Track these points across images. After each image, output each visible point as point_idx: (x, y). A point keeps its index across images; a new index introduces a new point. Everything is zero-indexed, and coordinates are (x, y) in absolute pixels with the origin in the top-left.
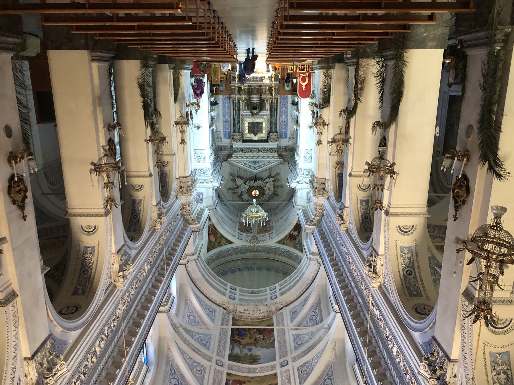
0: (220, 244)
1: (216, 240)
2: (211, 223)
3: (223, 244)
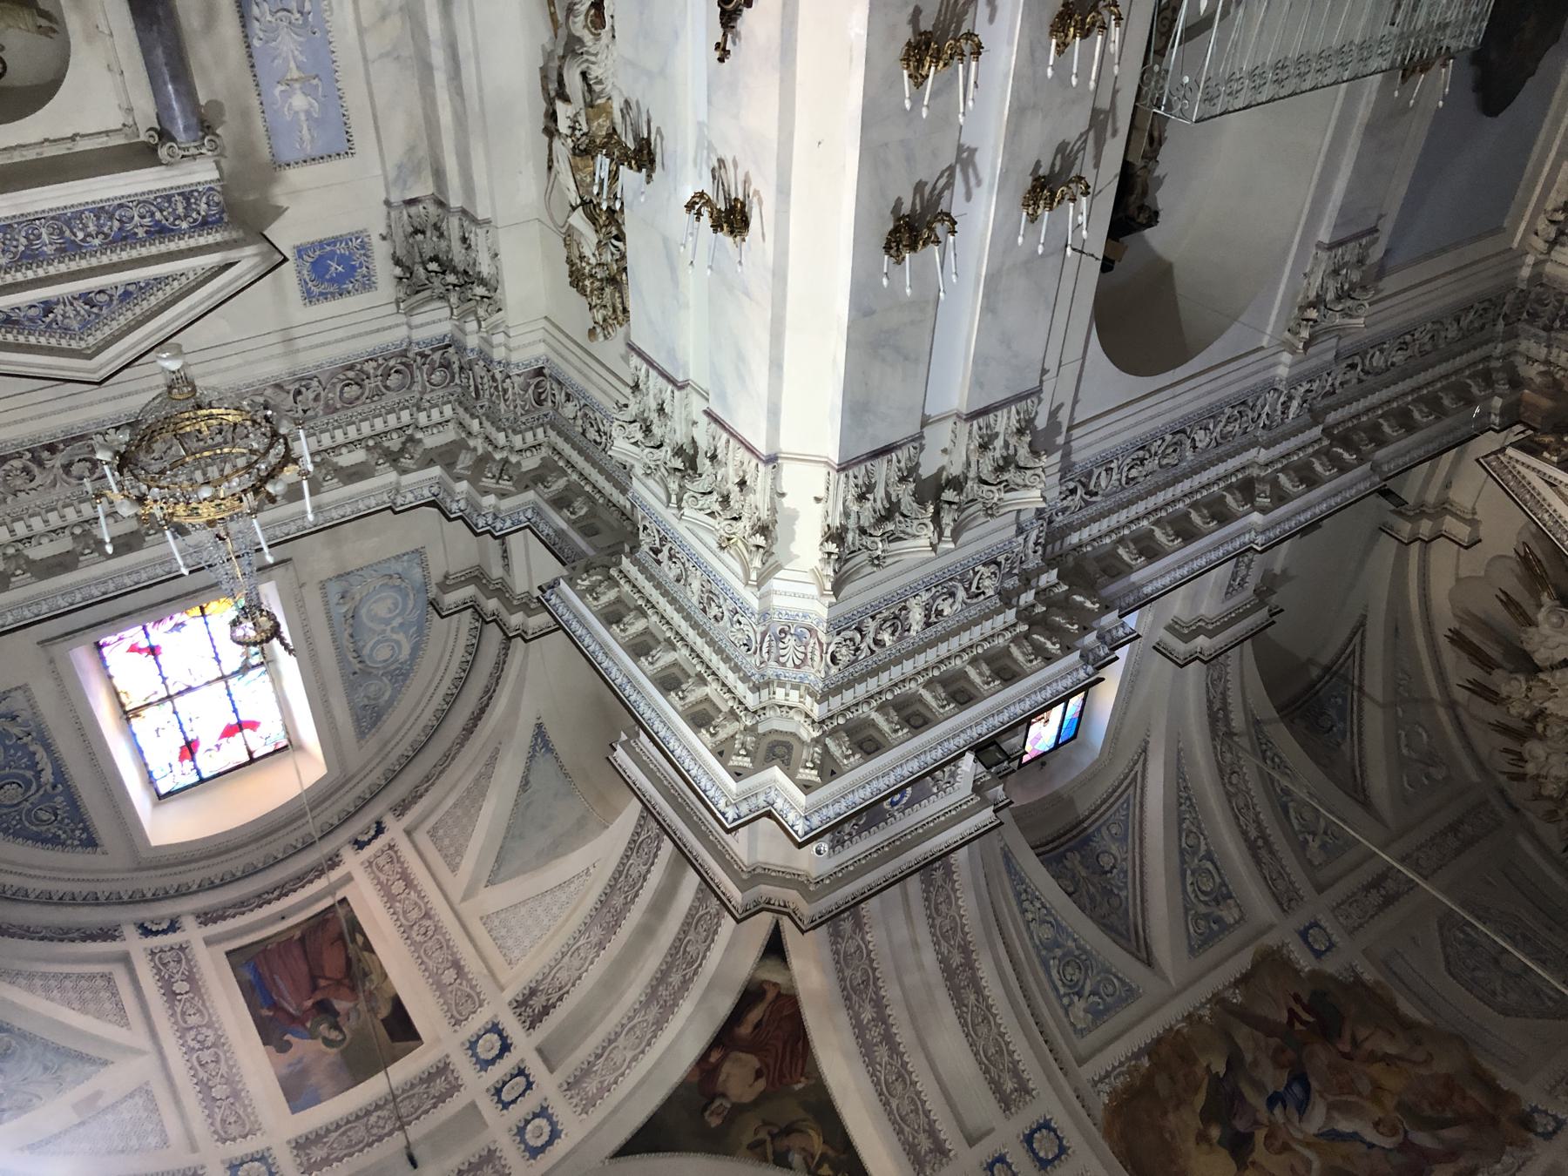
0: (786, 1142)
1: (762, 1099)
2: (772, 974)
3: (796, 1159)
